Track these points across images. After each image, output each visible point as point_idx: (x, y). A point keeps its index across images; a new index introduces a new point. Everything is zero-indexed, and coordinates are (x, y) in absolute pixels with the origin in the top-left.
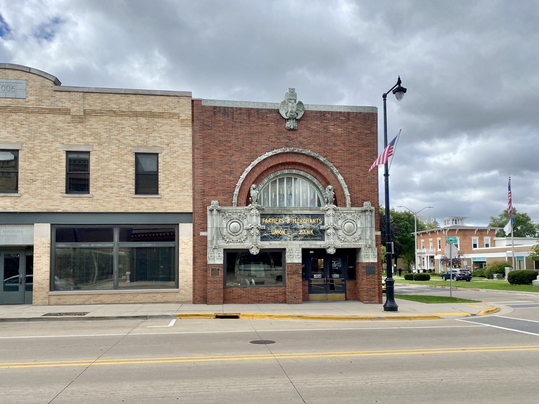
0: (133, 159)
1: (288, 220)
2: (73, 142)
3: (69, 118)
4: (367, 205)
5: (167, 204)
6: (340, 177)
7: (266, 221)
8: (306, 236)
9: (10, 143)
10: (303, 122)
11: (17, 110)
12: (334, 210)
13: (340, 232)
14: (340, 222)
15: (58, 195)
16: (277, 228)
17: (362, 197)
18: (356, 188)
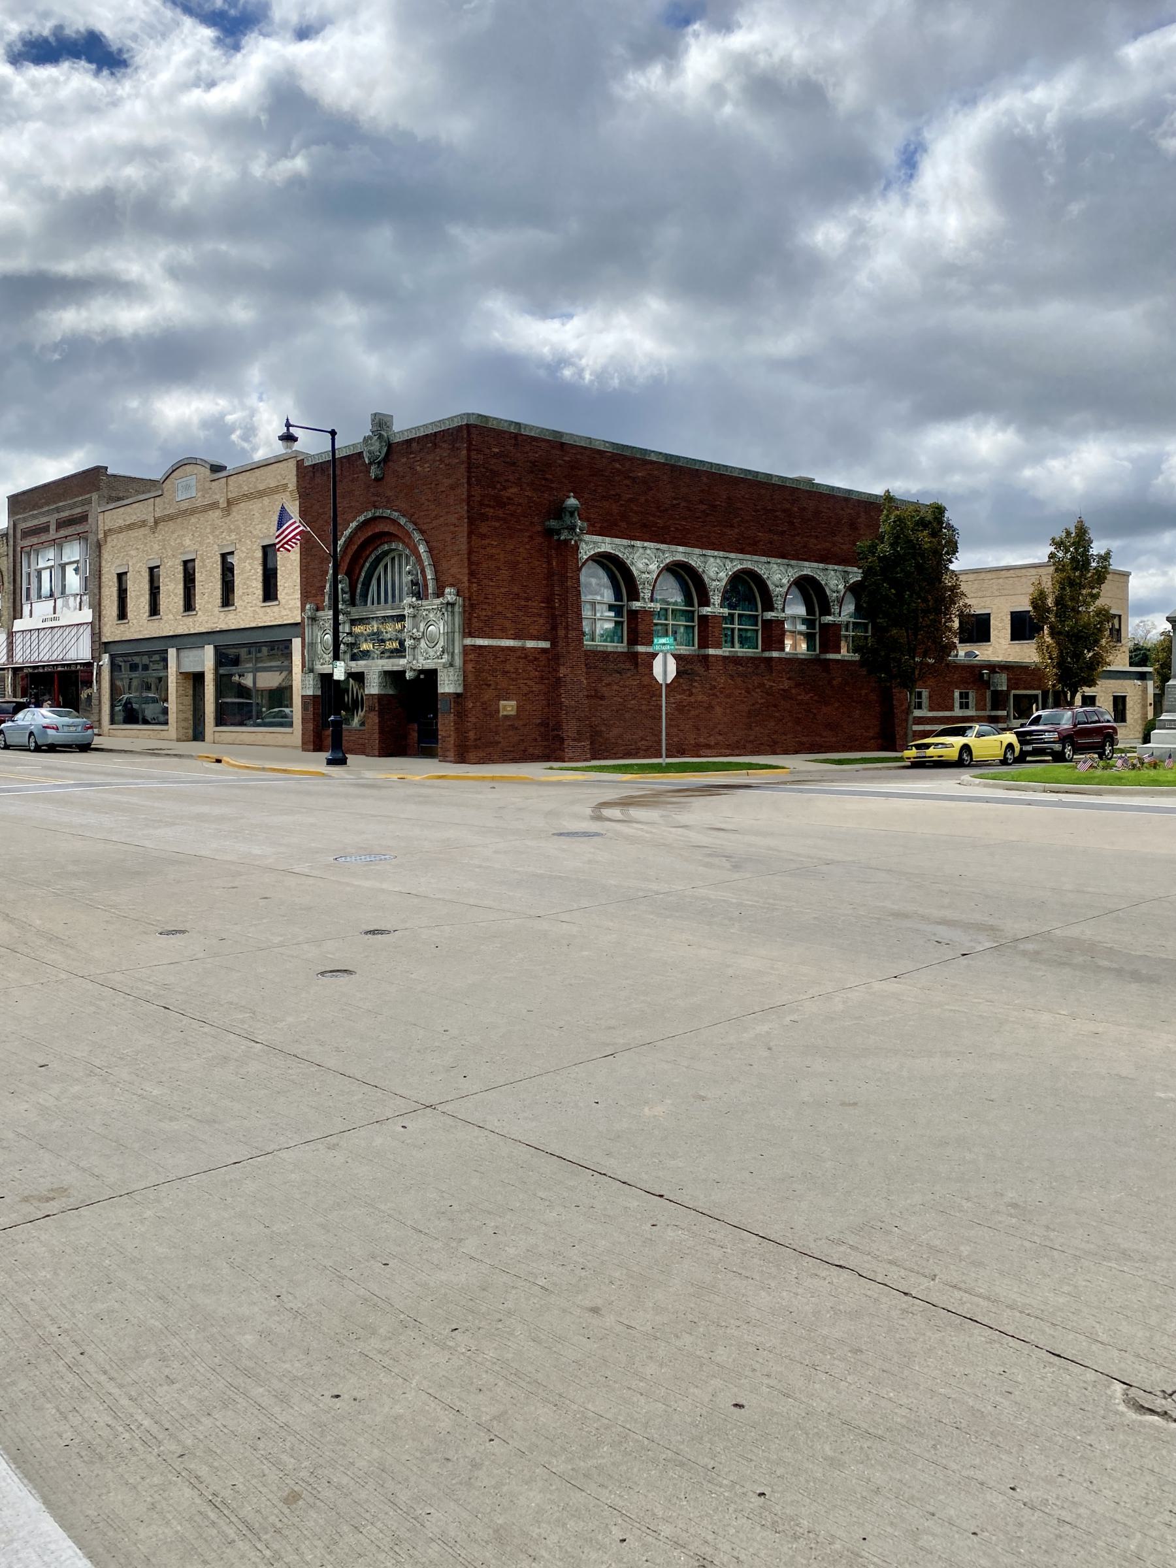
0: (259, 554)
1: (375, 626)
2: (225, 542)
3: (218, 513)
4: (450, 594)
5: (284, 613)
6: (422, 549)
7: (357, 630)
8: (392, 651)
9: (190, 552)
10: (390, 464)
11: (192, 512)
12: (411, 606)
13: (423, 644)
14: (422, 625)
15: (217, 609)
16: (366, 640)
17: (451, 580)
18: (444, 565)
